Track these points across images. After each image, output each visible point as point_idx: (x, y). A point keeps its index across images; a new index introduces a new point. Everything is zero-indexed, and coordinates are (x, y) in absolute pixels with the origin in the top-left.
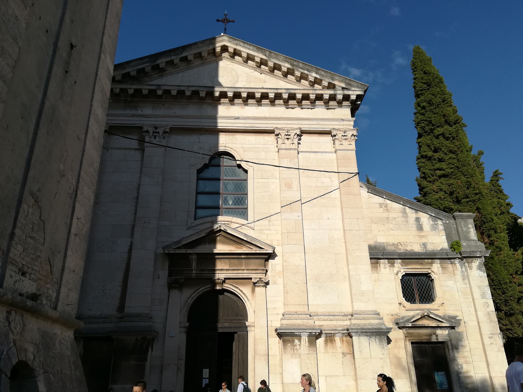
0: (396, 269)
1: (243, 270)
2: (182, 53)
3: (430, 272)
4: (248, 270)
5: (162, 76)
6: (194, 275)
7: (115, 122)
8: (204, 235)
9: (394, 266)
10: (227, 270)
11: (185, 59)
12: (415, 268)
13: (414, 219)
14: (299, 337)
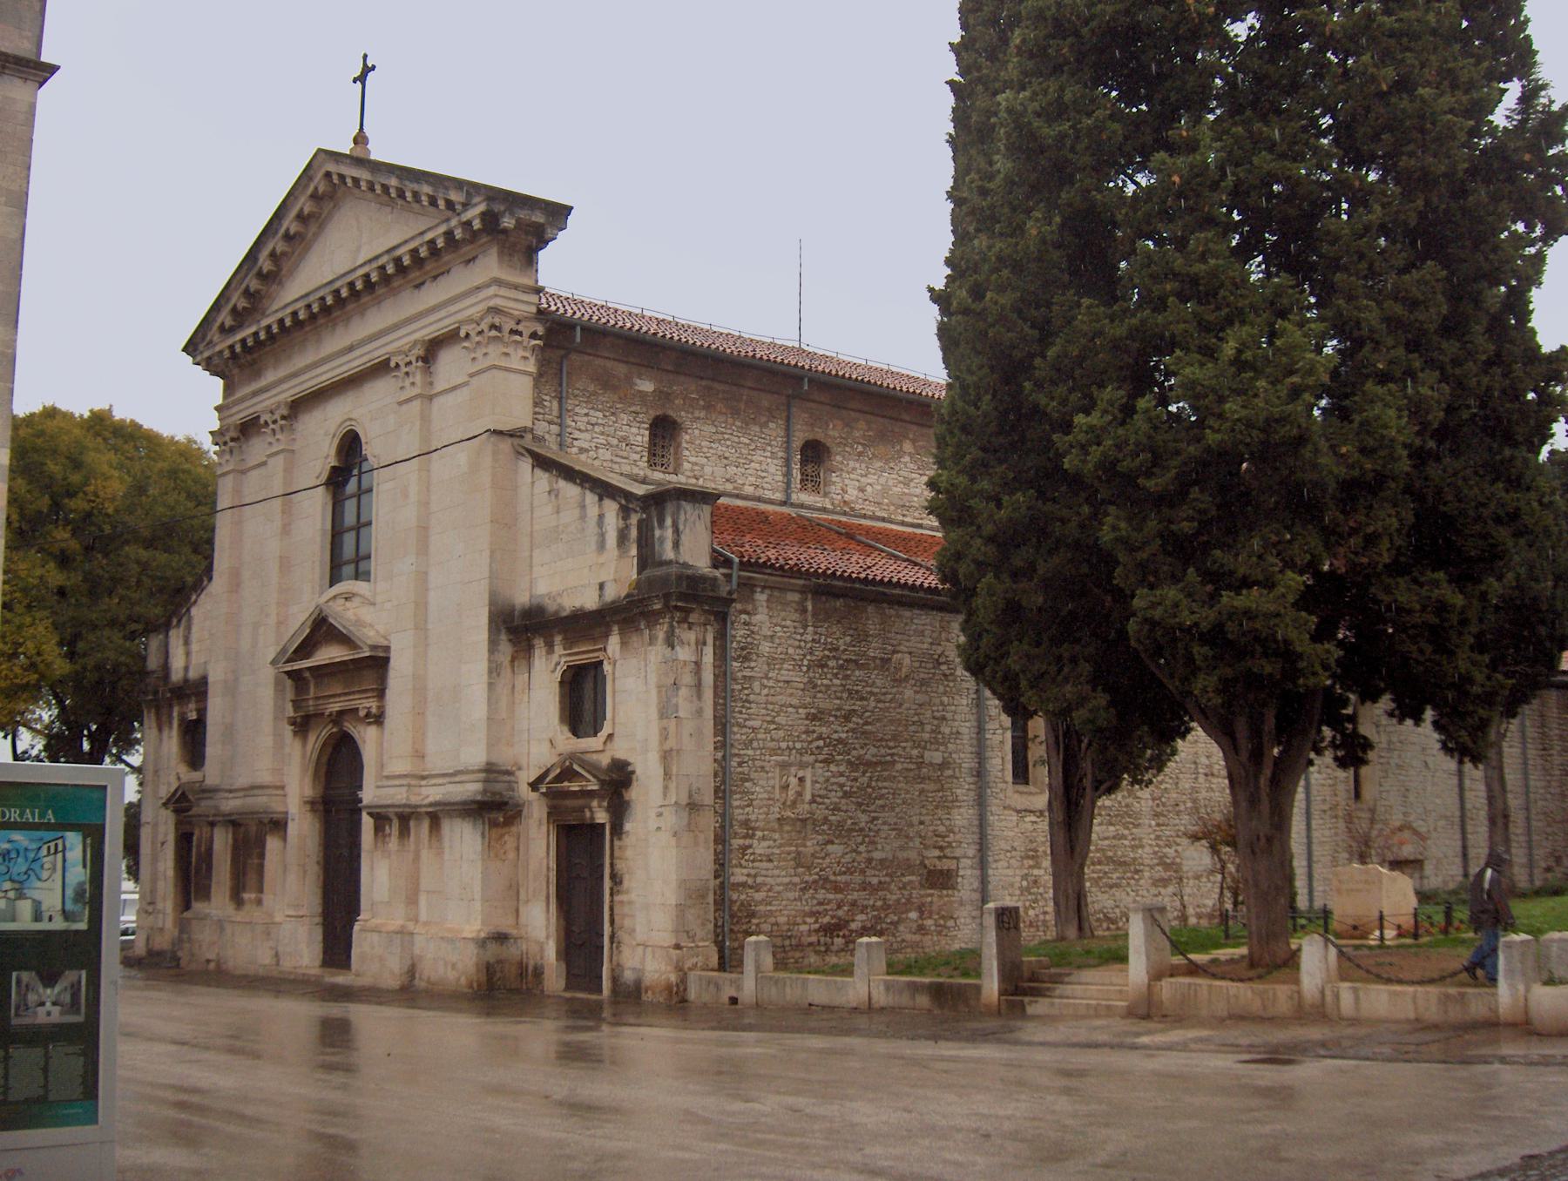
0: (555, 658)
1: (354, 693)
3: (601, 655)
4: (359, 692)
7: (242, 415)
8: (308, 631)
9: (553, 652)
10: (340, 695)
11: (288, 237)
12: (584, 652)
13: (596, 519)
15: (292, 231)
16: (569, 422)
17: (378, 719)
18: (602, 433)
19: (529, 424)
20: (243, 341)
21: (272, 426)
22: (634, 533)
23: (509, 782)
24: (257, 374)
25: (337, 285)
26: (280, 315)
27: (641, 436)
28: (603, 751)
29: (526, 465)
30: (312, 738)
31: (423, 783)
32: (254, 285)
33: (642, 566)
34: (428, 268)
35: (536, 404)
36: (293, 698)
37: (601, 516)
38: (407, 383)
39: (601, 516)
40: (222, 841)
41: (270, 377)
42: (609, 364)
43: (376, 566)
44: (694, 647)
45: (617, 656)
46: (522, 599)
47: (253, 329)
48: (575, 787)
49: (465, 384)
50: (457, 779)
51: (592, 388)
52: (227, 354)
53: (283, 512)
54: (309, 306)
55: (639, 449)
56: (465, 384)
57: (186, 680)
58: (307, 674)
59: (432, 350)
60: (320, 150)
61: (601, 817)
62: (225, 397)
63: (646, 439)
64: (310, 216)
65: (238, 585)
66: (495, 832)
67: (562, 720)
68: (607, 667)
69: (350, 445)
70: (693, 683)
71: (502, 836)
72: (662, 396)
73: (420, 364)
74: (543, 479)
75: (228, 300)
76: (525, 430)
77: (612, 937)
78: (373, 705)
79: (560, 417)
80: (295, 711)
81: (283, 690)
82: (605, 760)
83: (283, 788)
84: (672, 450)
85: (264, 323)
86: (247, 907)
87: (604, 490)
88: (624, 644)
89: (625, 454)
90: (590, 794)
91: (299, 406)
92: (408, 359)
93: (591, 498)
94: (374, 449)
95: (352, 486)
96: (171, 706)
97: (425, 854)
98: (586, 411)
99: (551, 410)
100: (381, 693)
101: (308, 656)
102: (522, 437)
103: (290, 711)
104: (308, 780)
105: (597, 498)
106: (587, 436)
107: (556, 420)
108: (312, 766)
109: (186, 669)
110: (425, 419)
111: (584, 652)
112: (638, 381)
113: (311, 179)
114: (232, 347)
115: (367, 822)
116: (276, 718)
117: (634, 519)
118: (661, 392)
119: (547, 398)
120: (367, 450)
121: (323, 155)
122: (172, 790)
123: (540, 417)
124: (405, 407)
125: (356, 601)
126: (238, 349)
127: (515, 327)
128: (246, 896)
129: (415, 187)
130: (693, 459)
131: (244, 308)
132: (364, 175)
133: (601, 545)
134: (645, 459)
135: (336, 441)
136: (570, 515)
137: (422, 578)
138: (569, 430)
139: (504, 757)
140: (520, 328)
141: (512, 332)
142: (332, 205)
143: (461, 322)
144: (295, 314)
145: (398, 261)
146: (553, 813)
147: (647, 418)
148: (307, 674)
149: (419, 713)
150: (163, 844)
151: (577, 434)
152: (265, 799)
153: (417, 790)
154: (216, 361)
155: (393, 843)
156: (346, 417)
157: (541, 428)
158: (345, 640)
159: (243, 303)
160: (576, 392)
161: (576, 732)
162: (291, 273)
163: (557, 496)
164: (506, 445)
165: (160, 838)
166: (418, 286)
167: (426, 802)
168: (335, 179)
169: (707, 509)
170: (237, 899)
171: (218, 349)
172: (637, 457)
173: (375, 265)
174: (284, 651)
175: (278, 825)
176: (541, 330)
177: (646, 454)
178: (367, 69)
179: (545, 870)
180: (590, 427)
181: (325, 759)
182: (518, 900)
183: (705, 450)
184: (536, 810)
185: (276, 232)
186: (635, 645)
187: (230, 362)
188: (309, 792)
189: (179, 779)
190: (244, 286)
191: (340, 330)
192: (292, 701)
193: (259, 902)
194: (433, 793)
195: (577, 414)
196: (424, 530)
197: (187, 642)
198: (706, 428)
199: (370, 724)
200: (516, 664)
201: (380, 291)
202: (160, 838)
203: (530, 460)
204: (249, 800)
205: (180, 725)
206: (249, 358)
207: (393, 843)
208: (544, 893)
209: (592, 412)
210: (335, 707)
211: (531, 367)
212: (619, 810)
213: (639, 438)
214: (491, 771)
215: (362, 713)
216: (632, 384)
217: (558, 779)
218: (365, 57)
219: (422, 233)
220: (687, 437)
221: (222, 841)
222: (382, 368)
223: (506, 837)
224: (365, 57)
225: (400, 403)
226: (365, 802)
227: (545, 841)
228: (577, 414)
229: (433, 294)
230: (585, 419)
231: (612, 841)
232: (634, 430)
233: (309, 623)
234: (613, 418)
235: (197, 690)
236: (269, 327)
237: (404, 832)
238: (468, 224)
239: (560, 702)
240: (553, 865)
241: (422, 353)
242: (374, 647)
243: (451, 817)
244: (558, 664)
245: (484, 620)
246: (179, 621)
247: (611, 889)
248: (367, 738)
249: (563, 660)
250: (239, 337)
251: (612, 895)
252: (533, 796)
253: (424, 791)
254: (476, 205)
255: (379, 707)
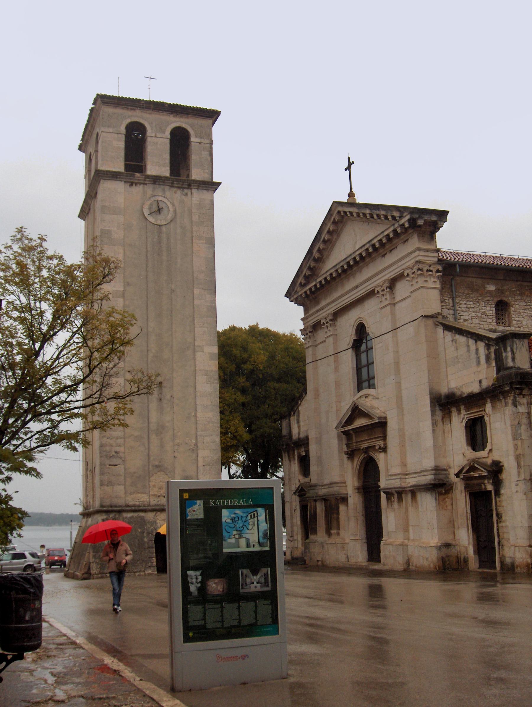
0: (462, 416)
1: (372, 439)
2: (321, 237)
4: (375, 438)
5: (324, 262)
6: (355, 447)
10: (366, 440)
11: (325, 242)
12: (475, 412)
13: (474, 351)
14: (393, 495)
15: (326, 239)
16: (458, 308)
17: (384, 449)
18: (474, 312)
19: (440, 311)
20: (310, 289)
21: (326, 325)
22: (493, 355)
23: (446, 474)
24: (318, 303)
25: (348, 260)
26: (325, 276)
27: (491, 311)
28: (488, 457)
29: (440, 330)
30: (356, 460)
31: (407, 477)
32: (312, 264)
33: (498, 370)
34: (387, 247)
35: (442, 302)
36: (346, 443)
37: (477, 350)
38: (383, 299)
39: (477, 350)
40: (320, 508)
41: (323, 303)
42: (474, 280)
43: (377, 381)
44: (526, 406)
45: (491, 413)
46: (444, 390)
47: (314, 283)
48: (476, 474)
49: (410, 296)
50: (422, 474)
51: (466, 291)
52: (304, 295)
53: (335, 362)
54: (337, 271)
55: (491, 317)
56: (410, 296)
57: (299, 439)
58: (351, 432)
59: (393, 283)
60: (334, 203)
61: (490, 487)
62: (305, 314)
63: (494, 312)
64: (333, 231)
65: (318, 396)
66: (442, 497)
67: (468, 444)
68: (486, 418)
69: (361, 329)
70: (527, 423)
71: (444, 499)
72: (500, 291)
73: (388, 290)
74: (449, 336)
75: (302, 272)
76: (438, 314)
77: (499, 543)
78: (381, 443)
79: (453, 306)
80: (347, 449)
81: (342, 440)
82: (489, 461)
83: (345, 483)
84: (507, 316)
85: (318, 280)
86: (333, 536)
87: (477, 337)
88: (493, 407)
89: (485, 320)
90: (484, 477)
91: (337, 315)
92: (382, 289)
93: (471, 342)
94: (372, 330)
95: (363, 347)
96: (294, 451)
97: (410, 509)
98: (465, 302)
99: (449, 304)
100: (384, 438)
101: (351, 424)
102: (437, 317)
103: (345, 449)
104: (356, 479)
105: (474, 342)
106: (467, 313)
107: (451, 308)
108: (357, 471)
109: (299, 433)
110: (393, 314)
111: (475, 412)
112: (488, 286)
113: (332, 215)
114: (306, 292)
115: (383, 496)
116: (340, 452)
117: (492, 349)
118: (499, 290)
119: (446, 298)
120: (368, 330)
121: (336, 204)
122: (297, 487)
123: (444, 307)
124: (383, 310)
125: (370, 398)
126: (308, 293)
127: (429, 268)
128: (332, 532)
129: (378, 212)
130: (517, 319)
131: (309, 275)
132: (354, 210)
133: (479, 363)
134: (495, 321)
135: (355, 328)
136: (463, 350)
137: (398, 385)
138: (458, 312)
139: (443, 463)
140: (431, 268)
141: (428, 271)
142: (342, 225)
143: (404, 269)
144: (331, 274)
145: (373, 246)
146: (467, 487)
147: (493, 302)
148: (351, 432)
149: (402, 445)
150: (295, 510)
151: (462, 313)
152: (338, 488)
153: (404, 480)
154: (299, 299)
155: (396, 505)
156: (358, 317)
157: (445, 312)
158: (366, 415)
159: (308, 273)
160: (460, 294)
161: (474, 449)
162: (328, 257)
163: (456, 342)
164: (430, 322)
165: (294, 508)
166: (384, 256)
167: (409, 485)
168: (342, 214)
169: (526, 341)
170: (329, 534)
171: (300, 294)
172: (491, 321)
173: (364, 249)
174: (340, 422)
175: (344, 499)
176: (440, 269)
177: (495, 319)
178: (350, 164)
179: (465, 514)
180: (467, 309)
181: (362, 469)
182: (454, 528)
183: (522, 314)
184: (459, 486)
185: (320, 239)
186: (498, 407)
187: (306, 299)
188: (356, 484)
189: (300, 482)
190: (308, 265)
191: (352, 279)
192: (346, 444)
193: (338, 534)
194: (411, 481)
195: (461, 304)
196: (397, 364)
197: (298, 422)
198: (521, 304)
199: (381, 452)
200: (444, 420)
201: (367, 260)
202: (294, 508)
203: (442, 327)
204: (331, 489)
205: (298, 458)
206: (313, 296)
207: (396, 505)
208: (466, 524)
209: (468, 303)
210: (365, 445)
211: (438, 285)
212: (498, 484)
213: (491, 312)
214: (437, 470)
215: (377, 447)
216: (485, 288)
217: (468, 471)
218: (349, 158)
219: (383, 232)
220: (513, 309)
221: (320, 508)
222: (371, 294)
223: (447, 499)
224: (349, 158)
225: (381, 308)
226: (382, 487)
227: (464, 500)
228: (461, 304)
229: (390, 259)
230: (465, 306)
231: (495, 498)
232: (488, 308)
233: (350, 409)
234: (478, 304)
235: (304, 442)
236: (320, 282)
237: (400, 499)
238: (403, 225)
239: (466, 436)
240: (469, 511)
241: (388, 285)
242: (380, 418)
243: (421, 492)
244: (463, 419)
245: (428, 402)
246: (294, 413)
247: (497, 521)
248: (380, 458)
249: (466, 416)
250: (308, 287)
251: (497, 523)
252: (457, 480)
253: (408, 480)
254: (405, 216)
255: (384, 444)
